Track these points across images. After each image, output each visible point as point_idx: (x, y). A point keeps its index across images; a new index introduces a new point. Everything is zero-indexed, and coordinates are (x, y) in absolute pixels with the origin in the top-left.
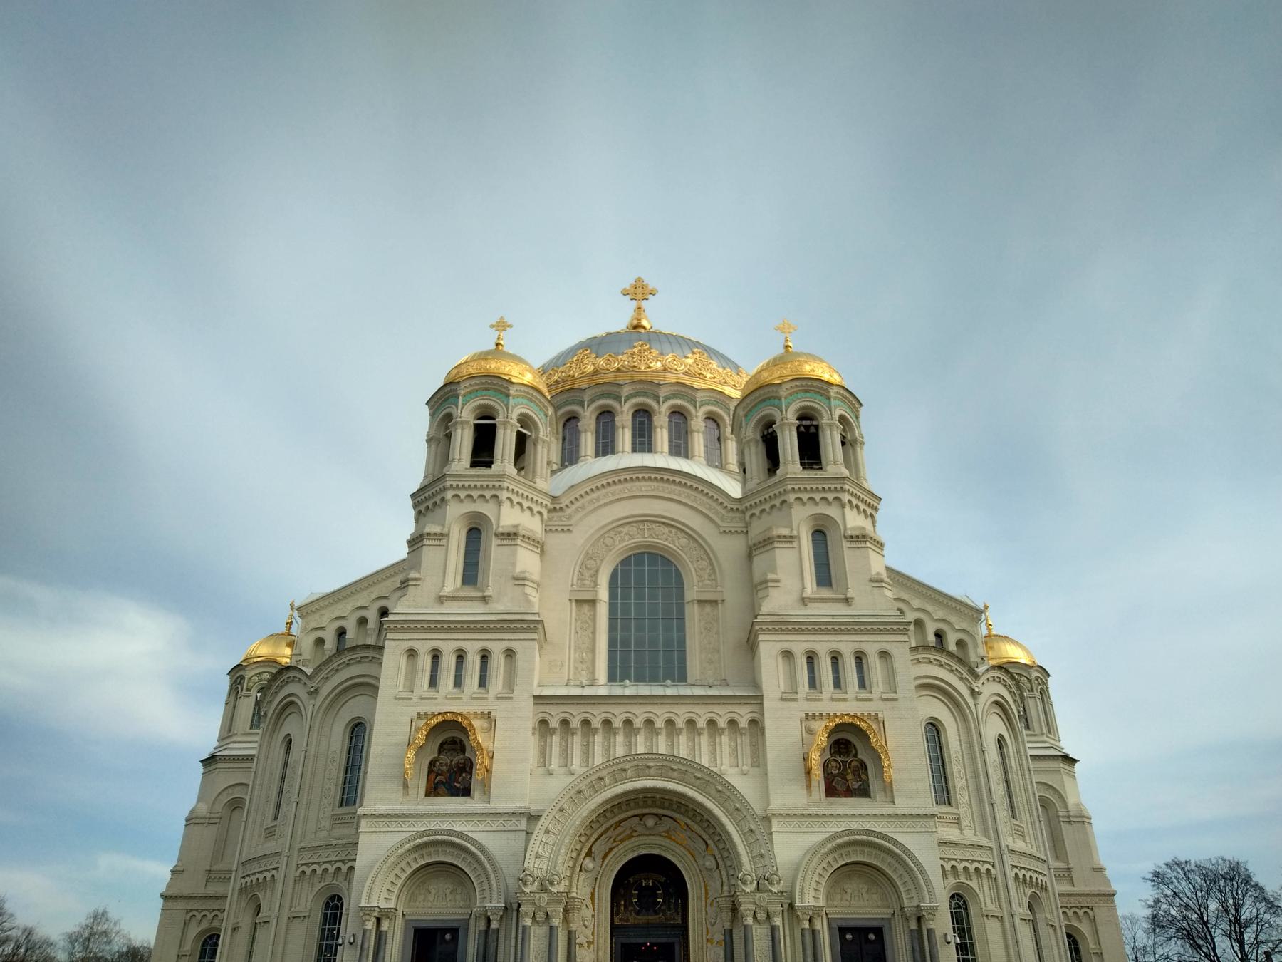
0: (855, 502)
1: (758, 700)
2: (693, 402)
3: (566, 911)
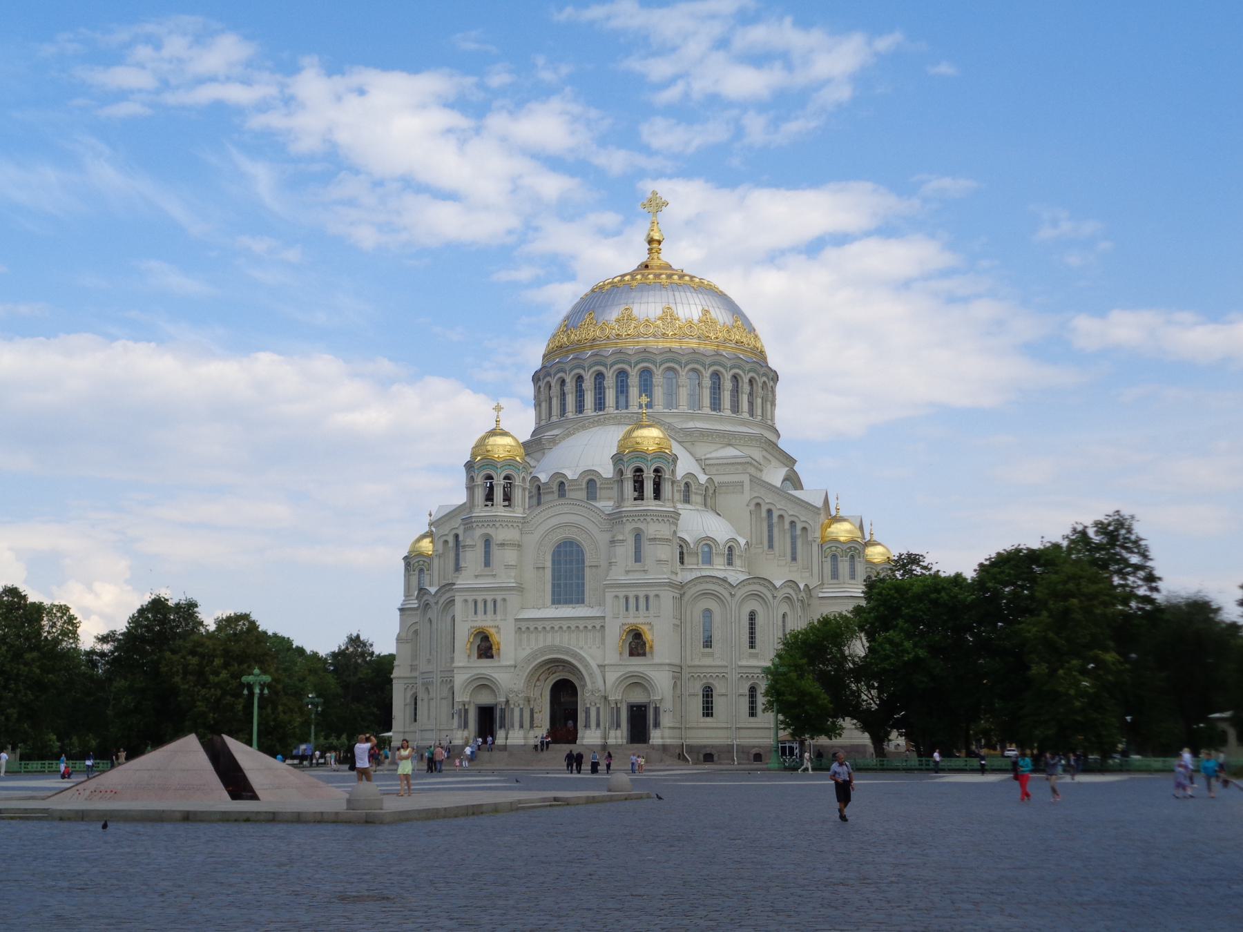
2: (654, 363)
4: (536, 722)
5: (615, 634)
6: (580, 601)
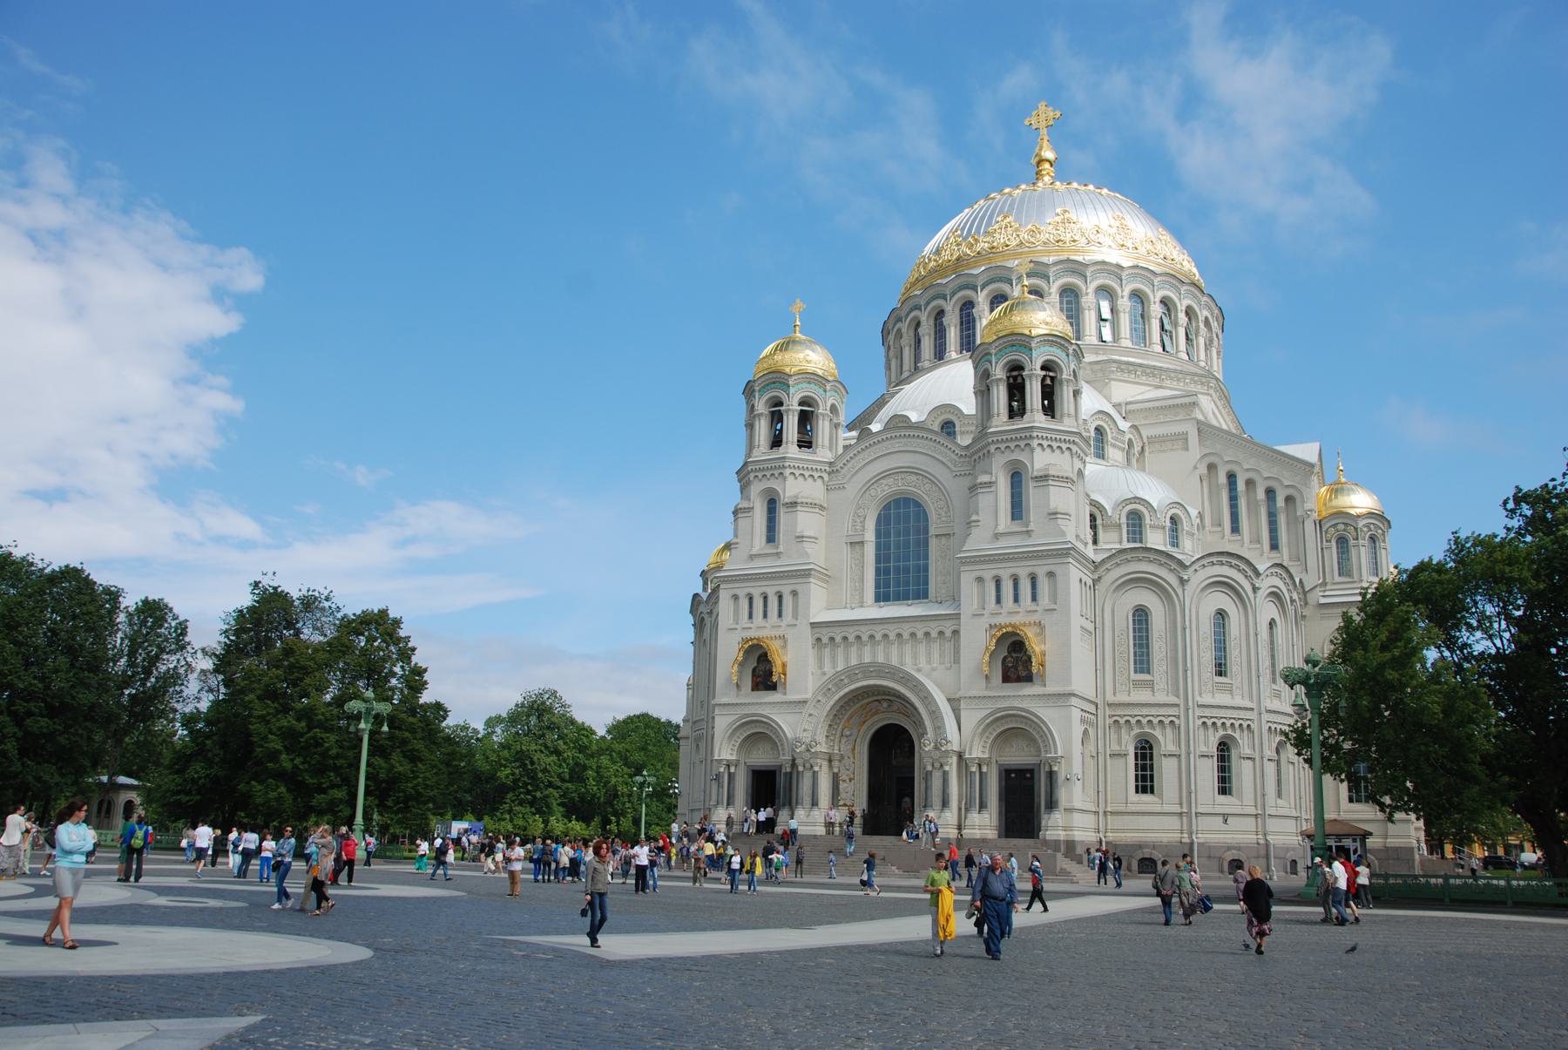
0: (1045, 443)
1: (957, 616)
3: (830, 761)
4: (844, 796)
5: (977, 643)
6: (922, 594)
